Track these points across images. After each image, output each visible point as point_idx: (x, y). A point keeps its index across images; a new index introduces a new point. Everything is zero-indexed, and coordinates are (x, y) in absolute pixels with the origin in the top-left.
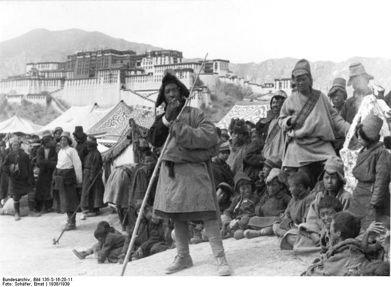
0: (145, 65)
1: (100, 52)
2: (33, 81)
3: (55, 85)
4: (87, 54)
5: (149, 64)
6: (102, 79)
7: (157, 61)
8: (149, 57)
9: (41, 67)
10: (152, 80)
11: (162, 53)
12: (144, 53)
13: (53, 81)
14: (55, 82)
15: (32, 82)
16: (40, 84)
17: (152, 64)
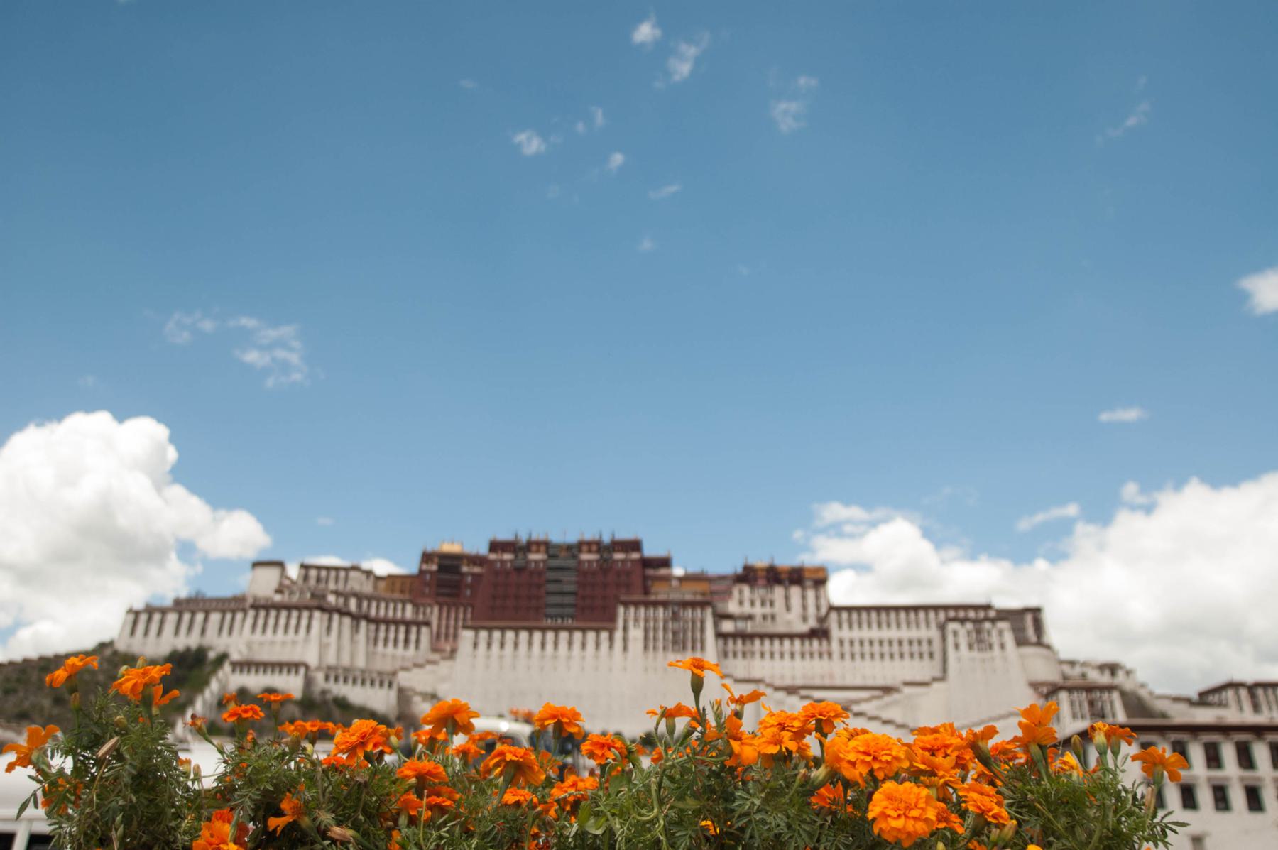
0: (747, 609)
1: (594, 548)
2: (336, 617)
3: (407, 641)
4: (534, 548)
5: (763, 604)
6: (636, 634)
7: (787, 598)
8: (761, 582)
9: (312, 582)
10: (830, 655)
11: (807, 575)
12: (740, 570)
13: (402, 629)
14: (407, 632)
15: (330, 620)
16: (356, 629)
17: (772, 604)
